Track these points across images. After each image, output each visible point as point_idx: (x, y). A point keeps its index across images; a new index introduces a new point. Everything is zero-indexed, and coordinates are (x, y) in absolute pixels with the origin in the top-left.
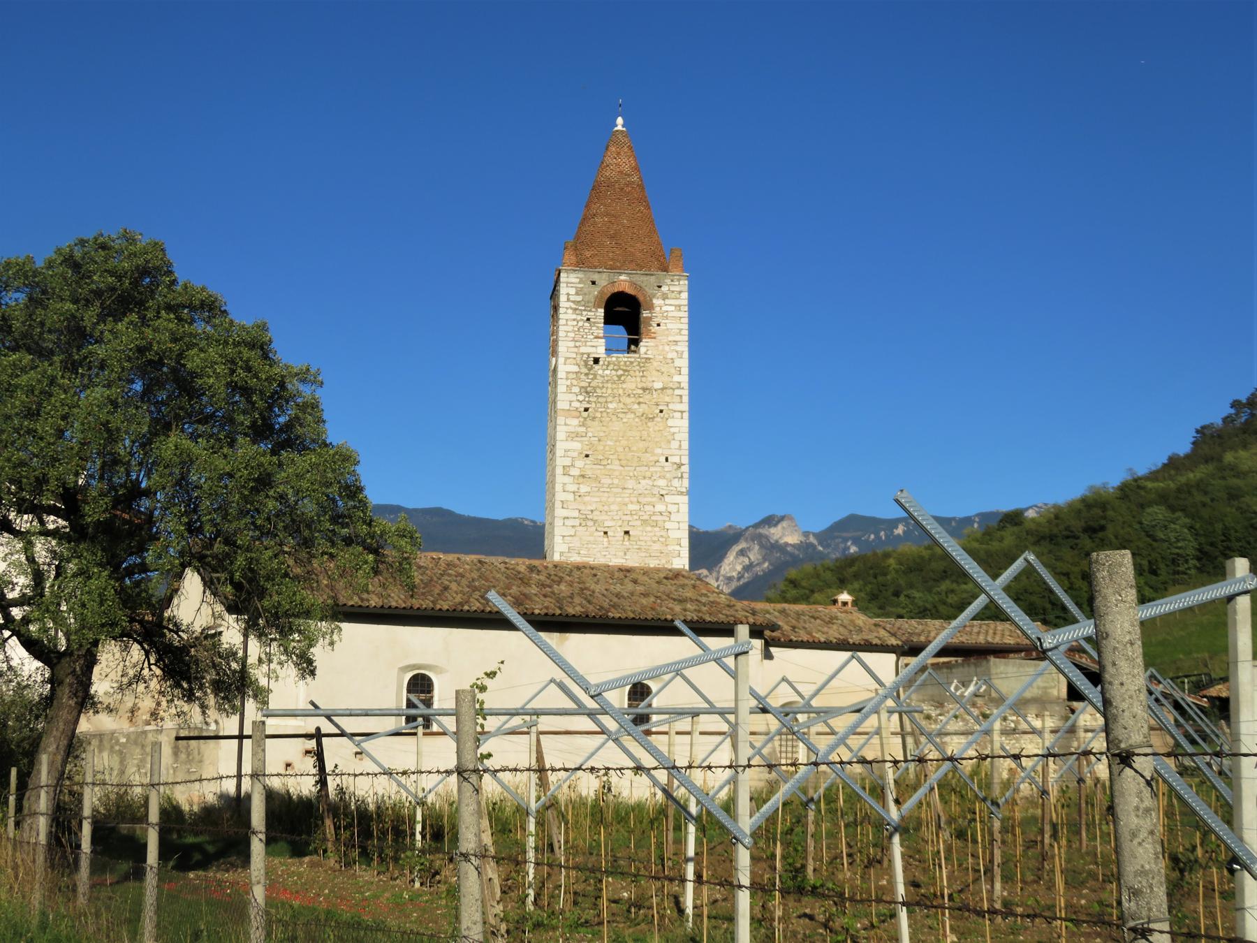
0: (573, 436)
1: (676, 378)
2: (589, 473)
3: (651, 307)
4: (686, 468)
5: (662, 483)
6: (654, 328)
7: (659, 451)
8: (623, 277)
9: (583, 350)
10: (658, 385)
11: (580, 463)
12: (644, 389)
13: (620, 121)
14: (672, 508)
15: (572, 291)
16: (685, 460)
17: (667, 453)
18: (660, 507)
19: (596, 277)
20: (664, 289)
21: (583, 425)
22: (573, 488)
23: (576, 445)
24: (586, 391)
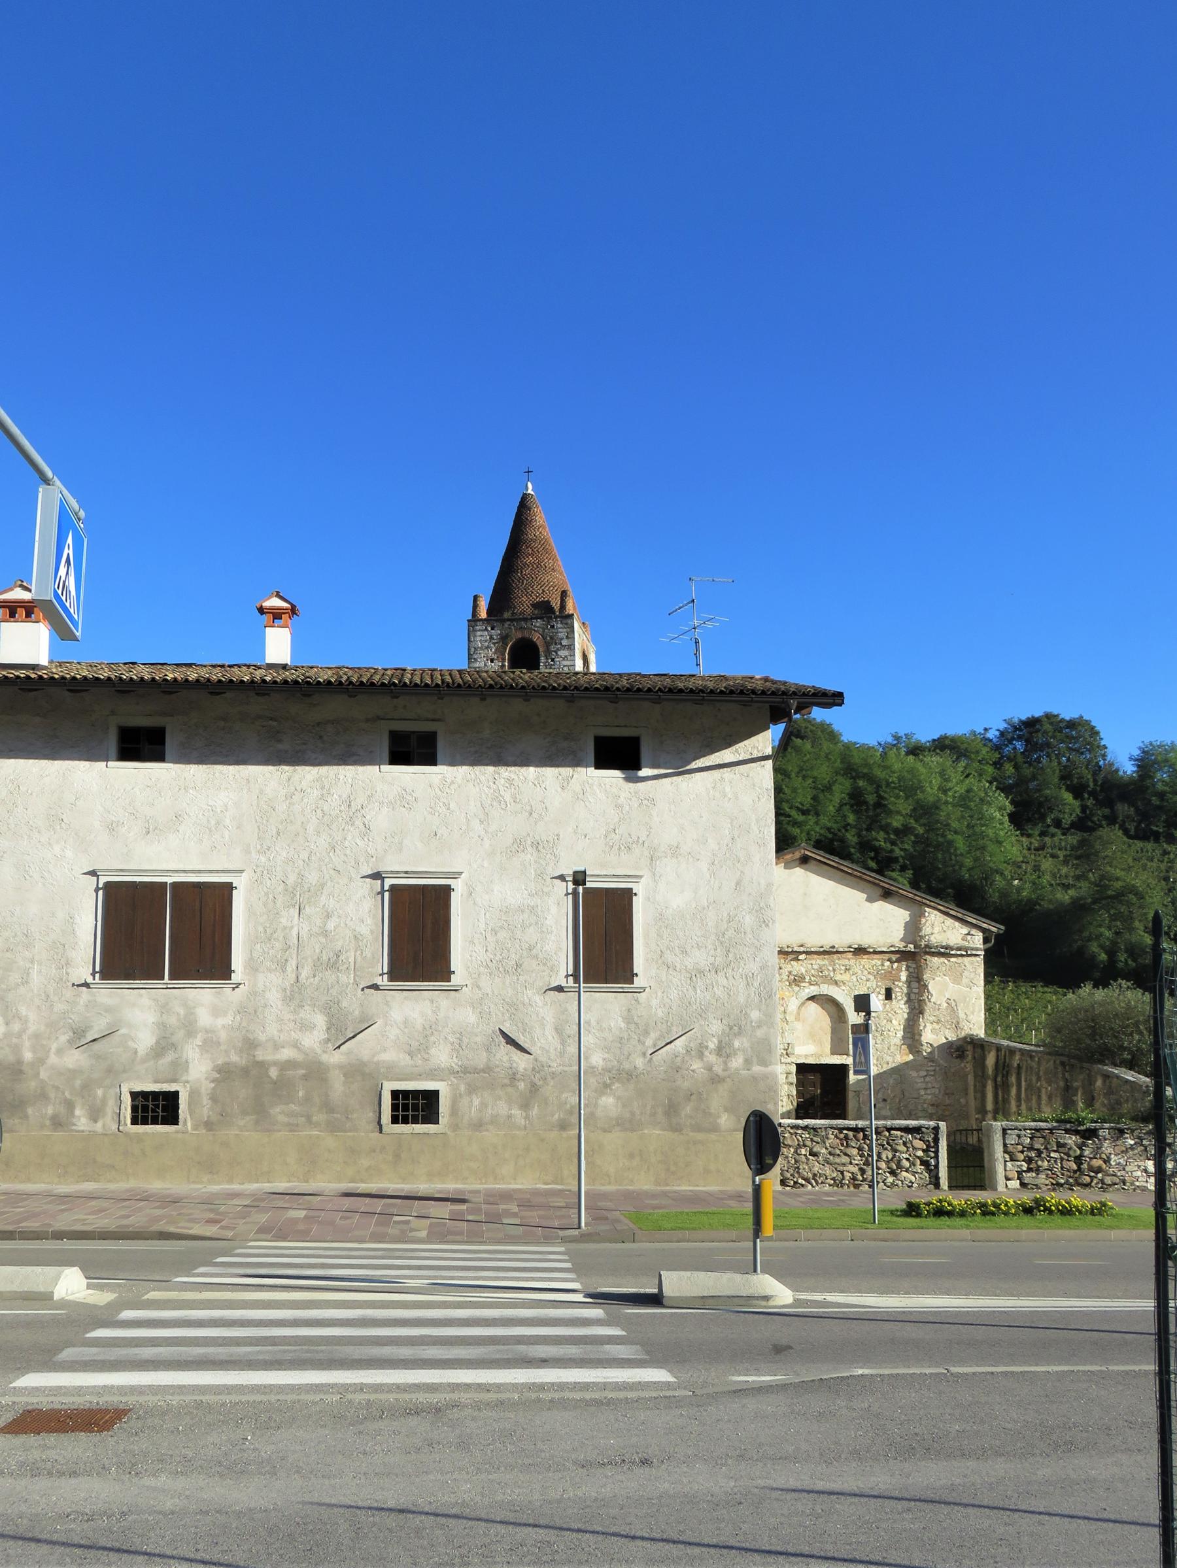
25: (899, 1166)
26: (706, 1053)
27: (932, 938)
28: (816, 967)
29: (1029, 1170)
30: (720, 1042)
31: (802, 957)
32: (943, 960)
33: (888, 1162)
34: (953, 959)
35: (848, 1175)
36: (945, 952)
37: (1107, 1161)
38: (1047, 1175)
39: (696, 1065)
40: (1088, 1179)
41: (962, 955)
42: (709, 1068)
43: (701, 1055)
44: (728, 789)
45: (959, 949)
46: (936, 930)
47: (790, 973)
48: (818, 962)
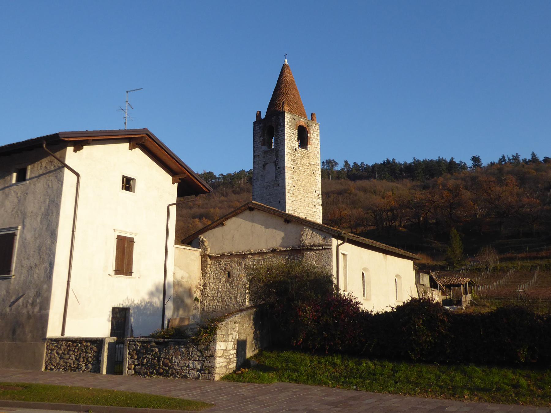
0: (291, 178)
1: (317, 161)
2: (295, 193)
3: (310, 133)
4: (320, 196)
5: (315, 200)
6: (311, 141)
7: (313, 188)
8: (302, 120)
9: (292, 145)
10: (313, 163)
11: (292, 189)
12: (309, 164)
13: (286, 60)
14: (318, 210)
15: (289, 121)
16: (321, 193)
17: (316, 189)
18: (314, 210)
19: (295, 117)
20: (313, 127)
21: (293, 174)
22: (291, 198)
23: (291, 182)
24: (293, 161)
25: (87, 359)
26: (28, 305)
27: (306, 242)
28: (256, 261)
29: (139, 365)
30: (33, 299)
31: (248, 256)
32: (312, 252)
33: (83, 358)
34: (317, 252)
35: (68, 364)
36: (311, 248)
37: (171, 361)
38: (145, 367)
39: (25, 311)
40: (162, 371)
41: (319, 249)
42: (28, 312)
43: (27, 306)
44: (50, 184)
45: (319, 246)
46: (309, 236)
47: (245, 264)
48: (257, 258)
